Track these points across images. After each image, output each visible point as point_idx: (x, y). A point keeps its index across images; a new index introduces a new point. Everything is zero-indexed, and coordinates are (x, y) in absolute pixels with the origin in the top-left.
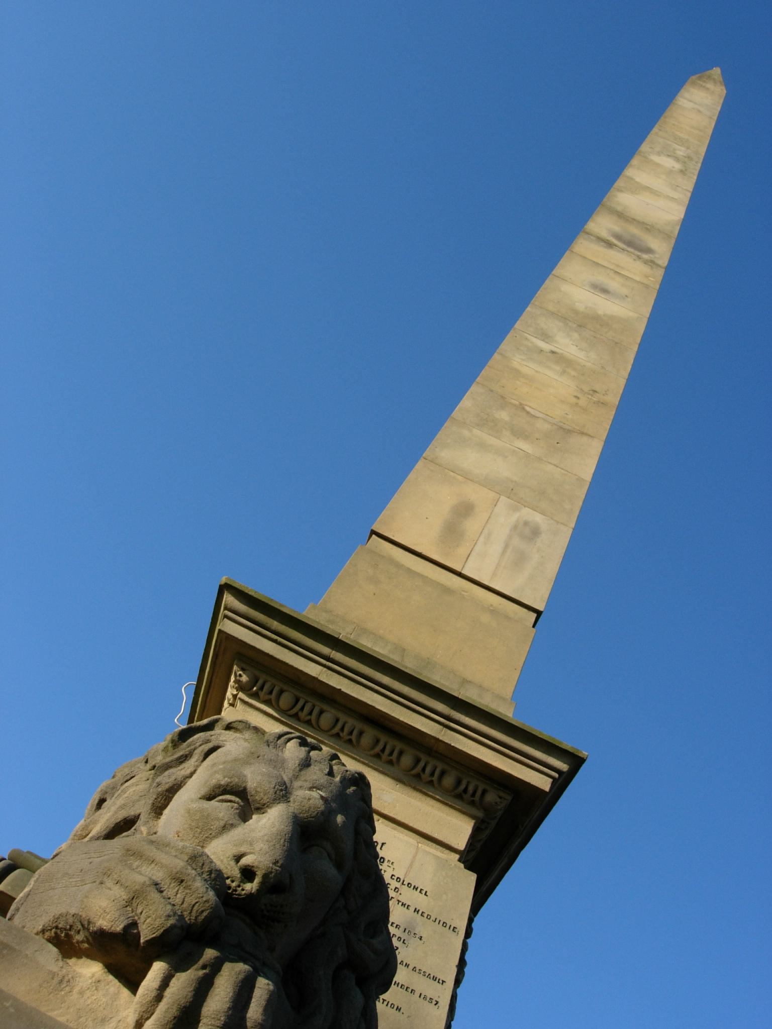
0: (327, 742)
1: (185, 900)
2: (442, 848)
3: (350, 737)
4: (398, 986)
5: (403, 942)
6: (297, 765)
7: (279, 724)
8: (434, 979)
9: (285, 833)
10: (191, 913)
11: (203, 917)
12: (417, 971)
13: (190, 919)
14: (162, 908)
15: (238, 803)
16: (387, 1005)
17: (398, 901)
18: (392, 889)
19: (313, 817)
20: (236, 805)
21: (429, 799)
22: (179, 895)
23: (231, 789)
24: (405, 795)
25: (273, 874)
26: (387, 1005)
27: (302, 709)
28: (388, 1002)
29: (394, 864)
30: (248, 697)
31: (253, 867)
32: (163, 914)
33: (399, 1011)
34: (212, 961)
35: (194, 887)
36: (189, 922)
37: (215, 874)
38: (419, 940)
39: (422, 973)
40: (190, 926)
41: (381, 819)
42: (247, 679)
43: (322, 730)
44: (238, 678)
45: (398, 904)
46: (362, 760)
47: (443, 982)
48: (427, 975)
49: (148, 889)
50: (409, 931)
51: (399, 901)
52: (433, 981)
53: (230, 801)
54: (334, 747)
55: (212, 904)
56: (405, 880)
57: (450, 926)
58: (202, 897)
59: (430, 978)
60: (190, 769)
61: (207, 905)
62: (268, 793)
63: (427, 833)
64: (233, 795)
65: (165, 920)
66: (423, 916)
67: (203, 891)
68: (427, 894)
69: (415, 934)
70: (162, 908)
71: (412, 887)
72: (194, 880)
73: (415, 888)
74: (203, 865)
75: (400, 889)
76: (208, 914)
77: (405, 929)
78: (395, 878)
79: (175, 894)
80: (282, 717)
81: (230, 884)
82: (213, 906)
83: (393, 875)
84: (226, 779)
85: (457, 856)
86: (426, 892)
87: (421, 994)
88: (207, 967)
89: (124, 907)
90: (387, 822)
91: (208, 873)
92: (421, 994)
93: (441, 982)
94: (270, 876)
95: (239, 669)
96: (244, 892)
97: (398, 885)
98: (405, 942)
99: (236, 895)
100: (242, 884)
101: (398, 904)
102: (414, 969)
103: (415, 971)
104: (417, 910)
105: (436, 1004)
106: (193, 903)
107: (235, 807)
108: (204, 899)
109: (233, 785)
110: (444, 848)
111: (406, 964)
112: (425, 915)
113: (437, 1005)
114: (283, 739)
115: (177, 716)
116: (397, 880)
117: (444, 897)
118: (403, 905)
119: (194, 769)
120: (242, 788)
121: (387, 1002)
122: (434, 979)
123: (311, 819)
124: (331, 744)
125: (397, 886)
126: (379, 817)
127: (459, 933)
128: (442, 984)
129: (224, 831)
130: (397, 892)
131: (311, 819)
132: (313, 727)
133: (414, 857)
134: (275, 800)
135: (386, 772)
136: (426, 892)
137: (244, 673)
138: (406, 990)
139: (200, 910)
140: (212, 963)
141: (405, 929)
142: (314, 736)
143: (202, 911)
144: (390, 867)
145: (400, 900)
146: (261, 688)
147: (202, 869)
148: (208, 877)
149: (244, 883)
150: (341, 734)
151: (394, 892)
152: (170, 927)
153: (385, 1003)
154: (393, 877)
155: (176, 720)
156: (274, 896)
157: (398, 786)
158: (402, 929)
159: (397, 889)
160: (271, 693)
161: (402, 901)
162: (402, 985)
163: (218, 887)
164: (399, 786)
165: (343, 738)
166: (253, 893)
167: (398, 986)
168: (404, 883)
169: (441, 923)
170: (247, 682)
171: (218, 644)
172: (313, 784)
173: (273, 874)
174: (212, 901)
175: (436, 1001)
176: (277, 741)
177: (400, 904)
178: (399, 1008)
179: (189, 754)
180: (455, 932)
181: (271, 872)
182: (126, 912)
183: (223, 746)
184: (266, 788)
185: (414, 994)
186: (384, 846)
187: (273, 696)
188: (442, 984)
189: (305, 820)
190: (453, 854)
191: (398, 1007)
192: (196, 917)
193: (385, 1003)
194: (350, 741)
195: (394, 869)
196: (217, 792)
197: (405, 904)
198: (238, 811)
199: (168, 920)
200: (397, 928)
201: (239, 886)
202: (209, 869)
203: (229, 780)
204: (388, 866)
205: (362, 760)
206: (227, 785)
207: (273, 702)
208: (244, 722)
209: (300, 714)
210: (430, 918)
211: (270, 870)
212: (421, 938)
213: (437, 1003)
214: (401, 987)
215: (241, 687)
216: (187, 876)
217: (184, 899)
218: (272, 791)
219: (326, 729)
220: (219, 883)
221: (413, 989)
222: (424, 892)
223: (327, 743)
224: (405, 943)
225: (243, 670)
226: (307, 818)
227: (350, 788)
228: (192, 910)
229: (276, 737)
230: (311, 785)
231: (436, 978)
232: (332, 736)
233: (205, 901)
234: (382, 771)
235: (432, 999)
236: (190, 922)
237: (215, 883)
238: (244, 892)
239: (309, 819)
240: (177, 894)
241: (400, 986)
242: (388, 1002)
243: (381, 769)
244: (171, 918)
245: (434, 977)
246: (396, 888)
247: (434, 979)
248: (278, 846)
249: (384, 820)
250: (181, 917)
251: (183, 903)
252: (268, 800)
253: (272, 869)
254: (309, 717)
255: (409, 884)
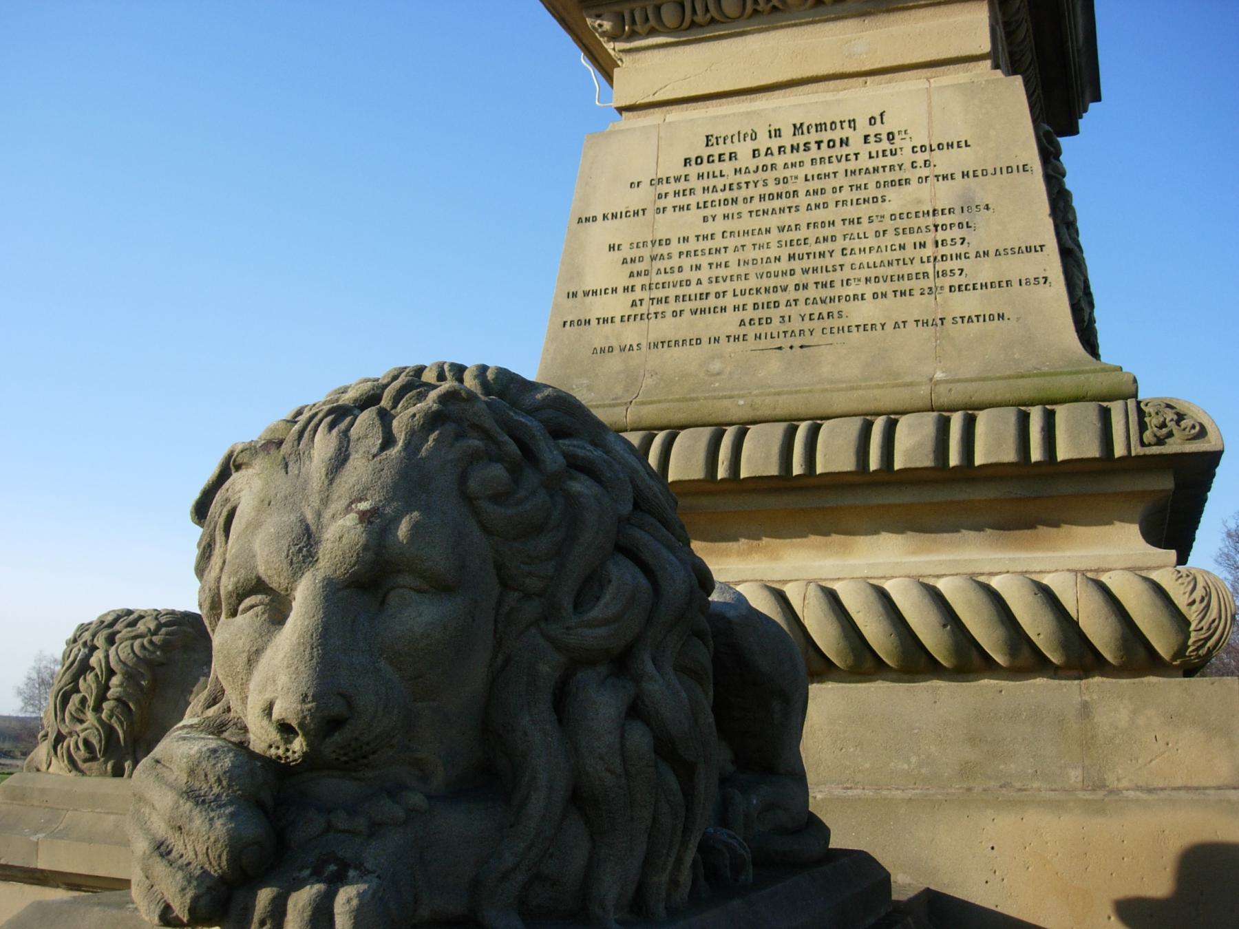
0: (749, 29)
1: (197, 849)
2: (963, 65)
3: (771, 4)
4: (986, 288)
5: (968, 227)
6: (324, 477)
7: (683, 47)
8: (1028, 250)
9: (309, 633)
10: (210, 863)
11: (225, 863)
12: (1002, 253)
13: (215, 871)
14: (171, 882)
15: (262, 604)
16: (984, 321)
17: (936, 176)
18: (921, 167)
19: (354, 566)
20: (260, 607)
21: (913, 11)
22: (188, 847)
23: (244, 589)
24: (881, 28)
25: (308, 718)
26: (984, 321)
27: (694, 11)
28: (984, 316)
29: (908, 132)
30: (628, 42)
31: (283, 719)
32: (175, 891)
33: (1003, 319)
34: (268, 909)
35: (194, 830)
36: (216, 875)
37: (225, 780)
38: (986, 210)
39: (1010, 252)
40: (222, 878)
41: (868, 78)
42: (610, 23)
43: (734, 19)
44: (600, 30)
45: (938, 180)
46: (803, 21)
47: (1041, 246)
48: (1017, 250)
49: (150, 861)
50: (968, 207)
51: (937, 176)
52: (1029, 254)
53: (252, 607)
54: (762, 28)
55: (225, 841)
56: (932, 143)
57: (1018, 167)
58: (209, 838)
59: (1022, 253)
60: (217, 565)
61: (220, 846)
62: (282, 570)
63: (933, 59)
64: (252, 595)
65: (182, 897)
66: (977, 176)
67: (205, 830)
68: (969, 143)
69: (977, 206)
70: (171, 882)
71: (945, 147)
72: (191, 821)
73: (950, 145)
74: (206, 775)
75: (931, 160)
76: (227, 855)
77: (962, 208)
78: (919, 149)
79: (184, 847)
80: (680, 37)
81: (276, 754)
82: (227, 843)
83: (913, 148)
84: (232, 579)
85: (988, 63)
86: (966, 141)
87: (1020, 280)
88: (266, 921)
89: (149, 890)
90: (877, 78)
91: (217, 784)
92: (1020, 280)
93: (1039, 249)
94: (306, 722)
95: (593, 20)
96: (296, 755)
97: (926, 156)
98: (970, 225)
99: (293, 761)
100: (288, 746)
101: (938, 180)
102: (997, 253)
103: (1000, 255)
104: (966, 173)
105: (1045, 283)
106: (204, 851)
107: (260, 613)
108: (212, 840)
109: (243, 583)
110: (966, 62)
111: (984, 252)
112: (979, 173)
113: (1048, 282)
114: (306, 435)
115: (595, 98)
116: (921, 151)
117: (993, 133)
118: (945, 177)
119: (222, 561)
120: (255, 580)
121: (982, 316)
122: (1029, 250)
123: (353, 569)
124: (756, 27)
125: (926, 159)
126: (864, 78)
127: (1033, 168)
128: (1042, 250)
129: (251, 668)
130: (930, 165)
131: (353, 569)
132: (723, 23)
133: (929, 106)
134: (295, 574)
135: (841, 15)
136: (966, 141)
137: (602, 20)
138: (1000, 286)
139: (216, 856)
140: (268, 912)
141: (962, 208)
142: (730, 32)
143: (220, 856)
144: (904, 139)
145: (938, 174)
146: (633, 22)
147: (208, 782)
148: (220, 787)
149: (291, 742)
150: (759, 8)
151: (925, 168)
152: (191, 902)
153: (981, 319)
154: (915, 149)
155: (597, 103)
156: (337, 734)
157: (866, 22)
158: (958, 210)
159: (928, 162)
160: (647, 19)
161: (941, 174)
162: (991, 283)
163: (240, 792)
164: (868, 21)
165: (763, 11)
166: (306, 751)
167: (986, 288)
168: (933, 148)
169: (1004, 170)
170: (613, 27)
171: (551, 9)
172: (350, 498)
173: (308, 718)
174: (223, 836)
175: (1043, 278)
176: (299, 444)
177: (940, 178)
178: (1001, 314)
179: (211, 540)
180: (1027, 171)
181: (305, 717)
182: (154, 894)
183: (239, 503)
184: (277, 565)
185: (1011, 286)
186: (884, 117)
187: (652, 22)
188: (1042, 250)
189: (346, 576)
190: (980, 63)
191: (999, 315)
192: (219, 865)
193: (981, 319)
194: (775, 9)
195: (911, 138)
196: (233, 603)
197: (947, 175)
198: (266, 616)
199: (184, 895)
200: (952, 213)
201: (287, 750)
202: (215, 778)
203: (236, 579)
204: (902, 139)
205: (803, 21)
206: (237, 588)
207: (657, 28)
208: (247, 449)
209: (697, 19)
210: (987, 172)
211: (301, 715)
212: (987, 207)
213: (1046, 279)
214: (992, 287)
215: (613, 38)
216: (180, 819)
217: (195, 850)
218: (285, 565)
219: (738, 15)
220: (238, 787)
221: (1008, 279)
222: (963, 144)
223: (751, 30)
224: (970, 227)
225: (598, 16)
226: (348, 572)
227: (428, 441)
228: (209, 860)
229: (295, 440)
230: (348, 501)
231: (1030, 247)
232: (751, 17)
233: (215, 842)
234: (835, 17)
235: (1038, 278)
236: (218, 873)
237: (233, 790)
238: (296, 755)
239: (350, 571)
240: (186, 846)
241: (989, 286)
242: (984, 316)
243: (833, 16)
244: (188, 890)
245: (1026, 248)
246: (925, 161)
247: (1028, 250)
248: (302, 668)
249: (873, 78)
250: (205, 873)
251: (196, 855)
252: (287, 581)
253: (303, 712)
254: (708, 16)
255: (939, 145)
